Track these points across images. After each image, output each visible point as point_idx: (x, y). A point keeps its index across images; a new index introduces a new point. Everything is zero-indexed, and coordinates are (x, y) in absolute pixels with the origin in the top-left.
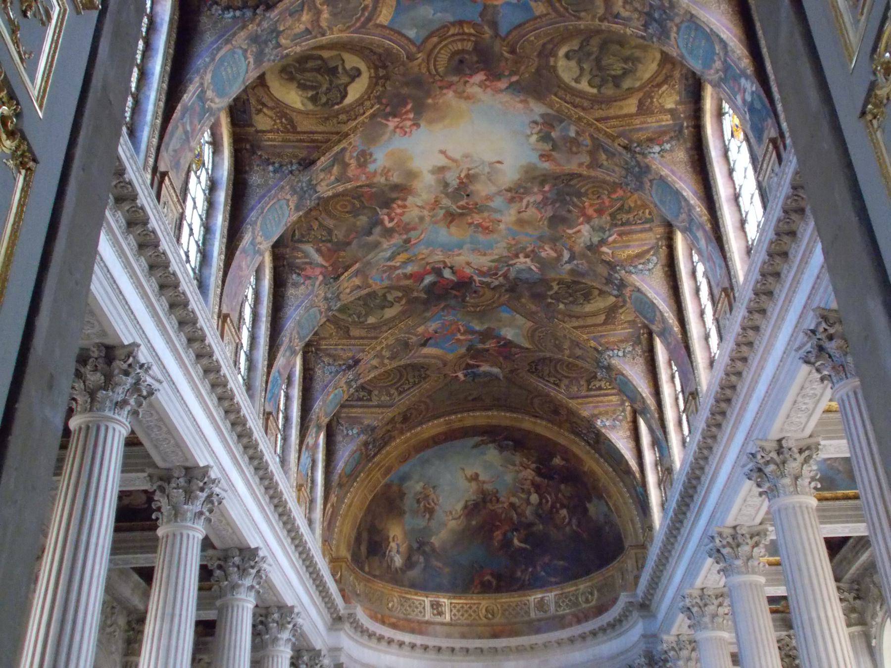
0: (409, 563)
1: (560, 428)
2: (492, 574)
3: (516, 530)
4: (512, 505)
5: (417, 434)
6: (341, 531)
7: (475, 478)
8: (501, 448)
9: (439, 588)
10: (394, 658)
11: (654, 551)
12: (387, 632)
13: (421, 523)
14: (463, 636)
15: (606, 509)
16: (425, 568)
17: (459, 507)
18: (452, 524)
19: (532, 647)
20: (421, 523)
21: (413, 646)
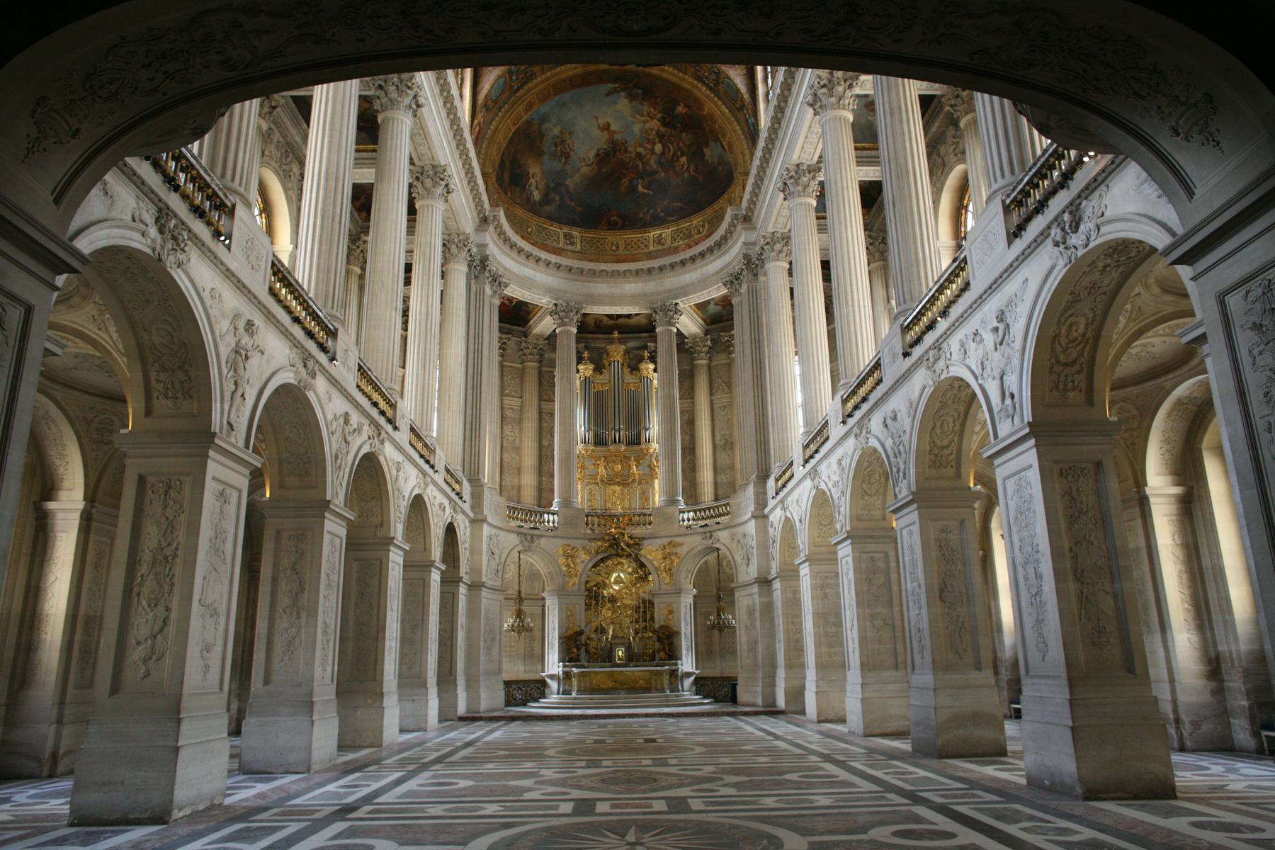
0: (546, 200)
1: (685, 73)
2: (618, 216)
3: (642, 178)
4: (638, 155)
5: (554, 75)
6: (486, 153)
7: (606, 127)
8: (632, 98)
9: (572, 223)
10: (532, 272)
11: (761, 144)
12: (527, 247)
13: (557, 165)
14: (591, 261)
15: (720, 150)
16: (560, 206)
17: (592, 154)
18: (585, 170)
19: (650, 271)
20: (557, 165)
21: (548, 264)
